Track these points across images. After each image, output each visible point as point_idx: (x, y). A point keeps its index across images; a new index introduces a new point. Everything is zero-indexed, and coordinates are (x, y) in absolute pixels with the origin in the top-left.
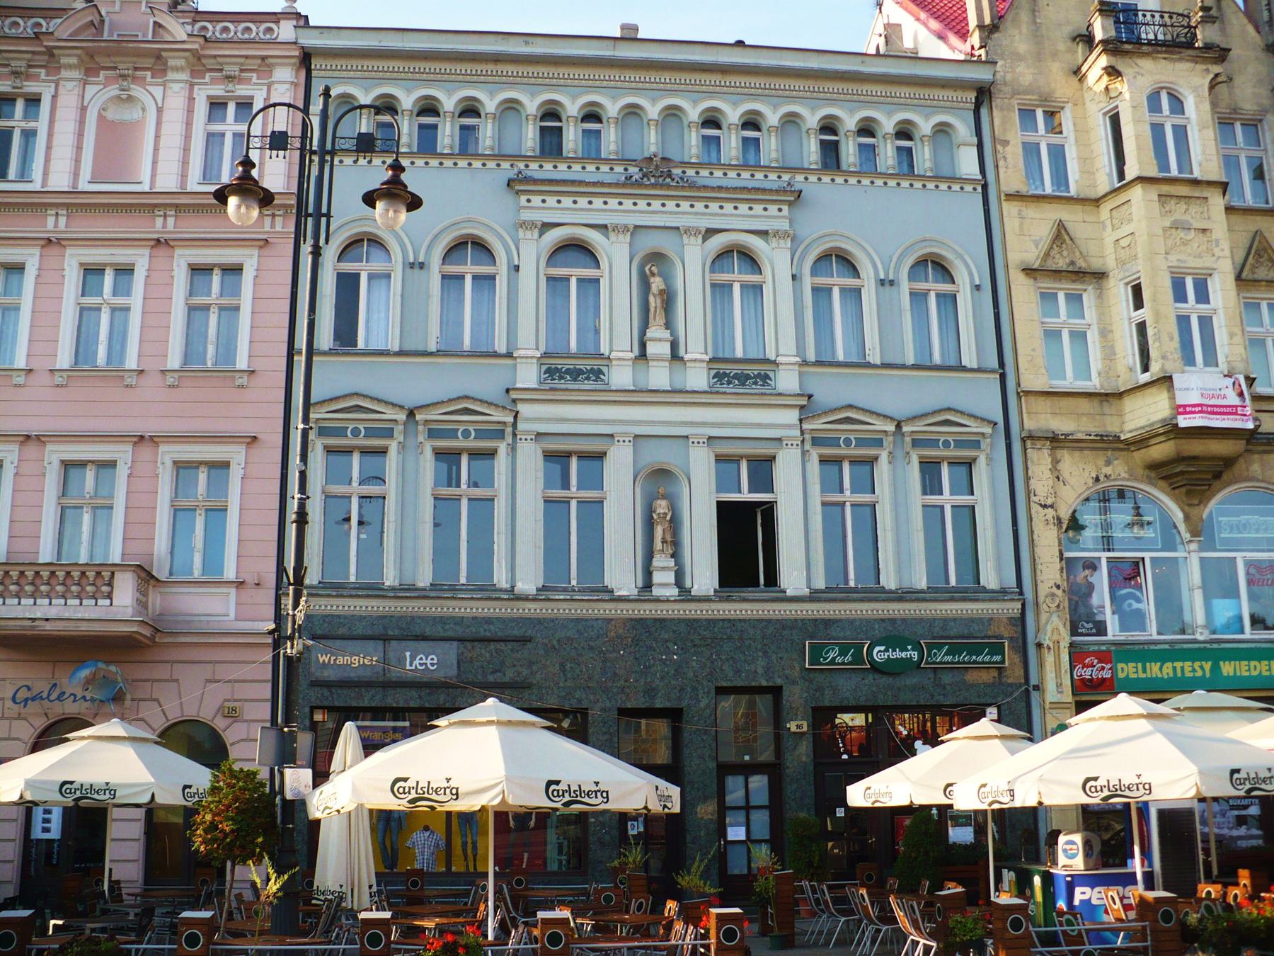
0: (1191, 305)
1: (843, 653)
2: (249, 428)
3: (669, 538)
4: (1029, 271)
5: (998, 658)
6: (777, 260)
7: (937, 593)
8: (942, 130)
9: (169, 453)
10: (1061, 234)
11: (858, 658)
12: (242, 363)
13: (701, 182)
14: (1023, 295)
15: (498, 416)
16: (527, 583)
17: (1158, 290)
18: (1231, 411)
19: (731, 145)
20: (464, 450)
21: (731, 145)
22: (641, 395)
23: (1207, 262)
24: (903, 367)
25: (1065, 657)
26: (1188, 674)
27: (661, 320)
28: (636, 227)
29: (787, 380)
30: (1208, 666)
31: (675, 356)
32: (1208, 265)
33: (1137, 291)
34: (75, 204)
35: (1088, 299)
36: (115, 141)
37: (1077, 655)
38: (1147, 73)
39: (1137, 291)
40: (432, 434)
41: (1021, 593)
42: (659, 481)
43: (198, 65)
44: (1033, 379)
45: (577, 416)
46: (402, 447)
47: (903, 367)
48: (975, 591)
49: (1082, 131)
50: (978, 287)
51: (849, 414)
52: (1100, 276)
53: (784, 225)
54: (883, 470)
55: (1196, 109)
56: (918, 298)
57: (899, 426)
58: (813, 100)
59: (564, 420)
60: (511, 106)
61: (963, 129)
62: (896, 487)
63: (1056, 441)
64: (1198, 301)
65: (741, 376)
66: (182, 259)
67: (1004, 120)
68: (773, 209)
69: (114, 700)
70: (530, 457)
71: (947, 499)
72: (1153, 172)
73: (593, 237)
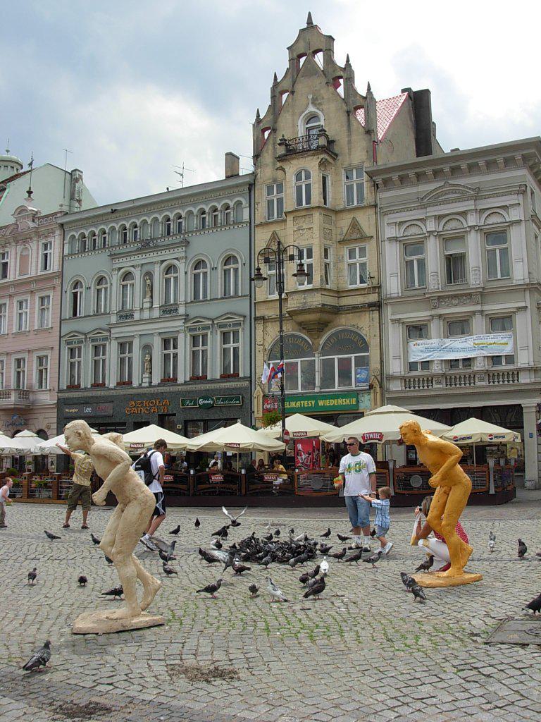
1: (191, 402)
2: (50, 344)
3: (148, 367)
5: (238, 402)
6: (181, 266)
8: (239, 204)
9: (36, 355)
11: (195, 404)
13: (160, 244)
16: (112, 386)
22: (142, 321)
23: (310, 241)
24: (217, 299)
25: (261, 401)
26: (306, 406)
27: (149, 295)
28: (142, 265)
29: (182, 310)
30: (313, 402)
31: (151, 308)
32: (310, 243)
41: (251, 377)
42: (147, 348)
43: (38, 234)
45: (126, 331)
46: (85, 346)
47: (217, 299)
50: (244, 264)
53: (183, 254)
57: (213, 322)
58: (194, 205)
59: (122, 332)
60: (113, 229)
61: (245, 203)
62: (214, 344)
64: (308, 258)
68: (180, 249)
69: (26, 425)
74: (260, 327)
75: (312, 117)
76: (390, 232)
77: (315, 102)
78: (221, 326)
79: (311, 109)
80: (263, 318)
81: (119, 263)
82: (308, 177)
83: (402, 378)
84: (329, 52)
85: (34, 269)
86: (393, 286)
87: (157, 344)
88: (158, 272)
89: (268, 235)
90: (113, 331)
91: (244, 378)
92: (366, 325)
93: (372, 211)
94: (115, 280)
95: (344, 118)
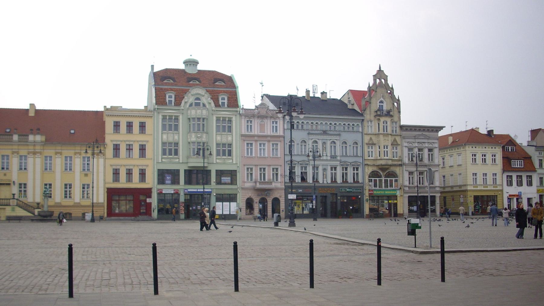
0: (386, 150)
6: (338, 143)
10: (371, 139)
12: (279, 156)
14: (366, 147)
17: (382, 147)
19: (333, 128)
21: (333, 128)
29: (339, 158)
34: (259, 136)
35: (373, 147)
36: (262, 127)
37: (369, 190)
38: (382, 119)
40: (301, 164)
44: (367, 157)
51: (345, 162)
52: (375, 144)
54: (349, 169)
56: (353, 147)
65: (334, 157)
66: (271, 143)
67: (365, 123)
70: (311, 167)
74: (366, 167)
75: (381, 102)
76: (406, 144)
77: (383, 96)
78: (353, 165)
79: (382, 99)
80: (367, 165)
81: (311, 137)
82: (386, 123)
84: (386, 80)
85: (268, 131)
86: (406, 160)
87: (329, 168)
91: (361, 183)
92: (397, 170)
93: (399, 137)
95: (392, 105)
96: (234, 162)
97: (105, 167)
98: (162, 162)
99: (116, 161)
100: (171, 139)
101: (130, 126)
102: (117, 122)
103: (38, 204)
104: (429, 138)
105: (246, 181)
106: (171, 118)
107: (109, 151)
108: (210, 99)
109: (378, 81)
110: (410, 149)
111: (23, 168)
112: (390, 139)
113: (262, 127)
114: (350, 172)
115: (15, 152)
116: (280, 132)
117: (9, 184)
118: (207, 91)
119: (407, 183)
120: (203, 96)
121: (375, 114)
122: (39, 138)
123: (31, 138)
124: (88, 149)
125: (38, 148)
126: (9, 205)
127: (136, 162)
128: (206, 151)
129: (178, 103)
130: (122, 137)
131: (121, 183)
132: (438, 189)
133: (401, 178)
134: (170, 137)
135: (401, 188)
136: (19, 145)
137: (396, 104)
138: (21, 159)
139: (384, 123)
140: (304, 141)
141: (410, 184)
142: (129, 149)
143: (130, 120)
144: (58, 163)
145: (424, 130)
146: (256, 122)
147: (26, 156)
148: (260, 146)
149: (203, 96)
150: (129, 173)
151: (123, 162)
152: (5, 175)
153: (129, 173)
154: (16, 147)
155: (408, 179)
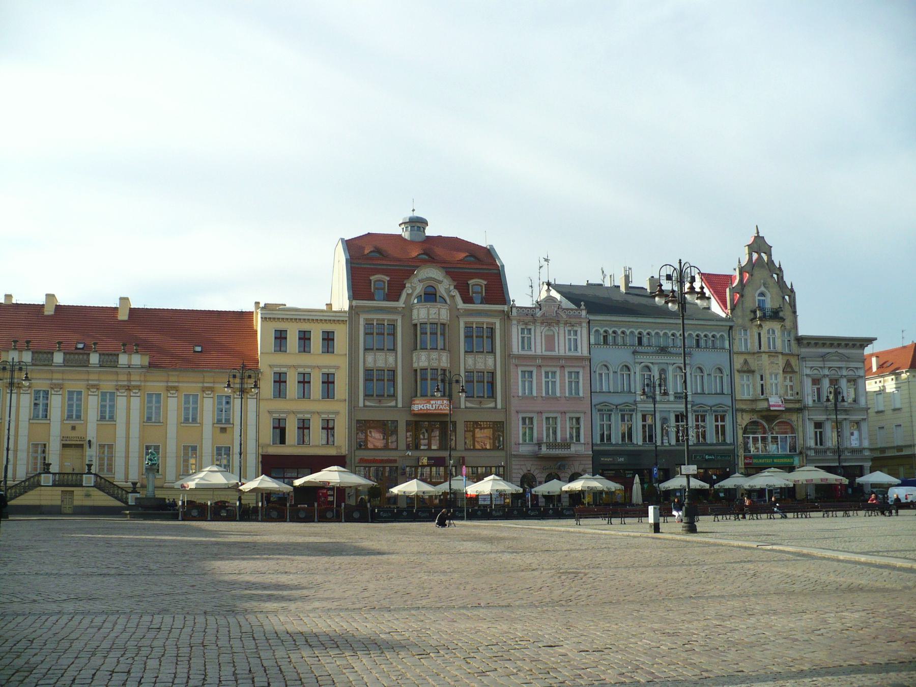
4: (738, 371)
7: (718, 444)
8: (722, 336)
10: (746, 362)
14: (737, 376)
15: (634, 407)
18: (780, 406)
20: (626, 413)
33: (762, 376)
34: (543, 358)
35: (750, 378)
36: (550, 342)
37: (745, 457)
38: (767, 325)
39: (762, 376)
42: (665, 420)
48: (727, 444)
49: (752, 336)
51: (701, 405)
52: (753, 372)
54: (708, 418)
55: (778, 333)
61: (726, 336)
62: (710, 423)
63: (743, 411)
66: (567, 370)
70: (640, 416)
71: (720, 423)
72: (767, 350)
73: (650, 365)
74: (739, 415)
75: (762, 294)
76: (808, 372)
77: (764, 284)
79: (763, 289)
81: (640, 358)
83: (814, 449)
84: (770, 255)
85: (562, 349)
86: (809, 401)
88: (671, 368)
89: (742, 361)
90: (639, 405)
91: (730, 444)
94: (638, 369)
96: (499, 406)
97: (258, 416)
98: (365, 406)
99: (280, 405)
100: (381, 364)
101: (305, 337)
102: (281, 331)
103: (134, 484)
104: (848, 359)
105: (521, 442)
106: (381, 324)
107: (267, 386)
108: (452, 287)
109: (755, 256)
110: (816, 381)
111: (107, 416)
112: (781, 361)
113: (550, 342)
114: (710, 423)
115: (93, 386)
116: (583, 351)
117: (81, 446)
118: (448, 273)
119: (811, 443)
120: (440, 282)
121: (752, 316)
122: (137, 360)
123: (123, 359)
124: (231, 380)
125: (136, 379)
126: (81, 486)
127: (316, 406)
128: (454, 385)
129: (394, 293)
130: (292, 359)
131: (290, 446)
132: (867, 453)
133: (801, 434)
134: (380, 360)
135: (801, 453)
136: (100, 372)
137: (787, 297)
138: (103, 400)
139: (769, 332)
140: (626, 366)
141: (816, 444)
142: (304, 381)
143: (305, 327)
144: (172, 406)
145: (839, 345)
146: (538, 331)
147: (112, 394)
148: (547, 377)
149: (440, 282)
150: (304, 426)
151: (292, 406)
152: (74, 428)
153: (304, 426)
154: (95, 377)
155: (813, 435)
